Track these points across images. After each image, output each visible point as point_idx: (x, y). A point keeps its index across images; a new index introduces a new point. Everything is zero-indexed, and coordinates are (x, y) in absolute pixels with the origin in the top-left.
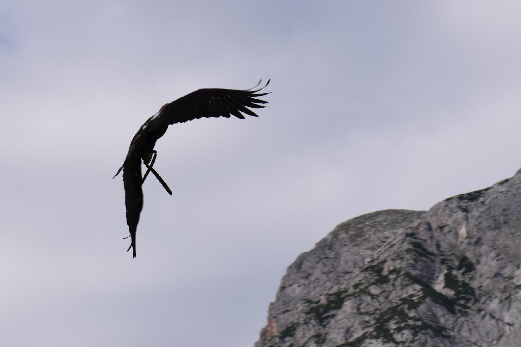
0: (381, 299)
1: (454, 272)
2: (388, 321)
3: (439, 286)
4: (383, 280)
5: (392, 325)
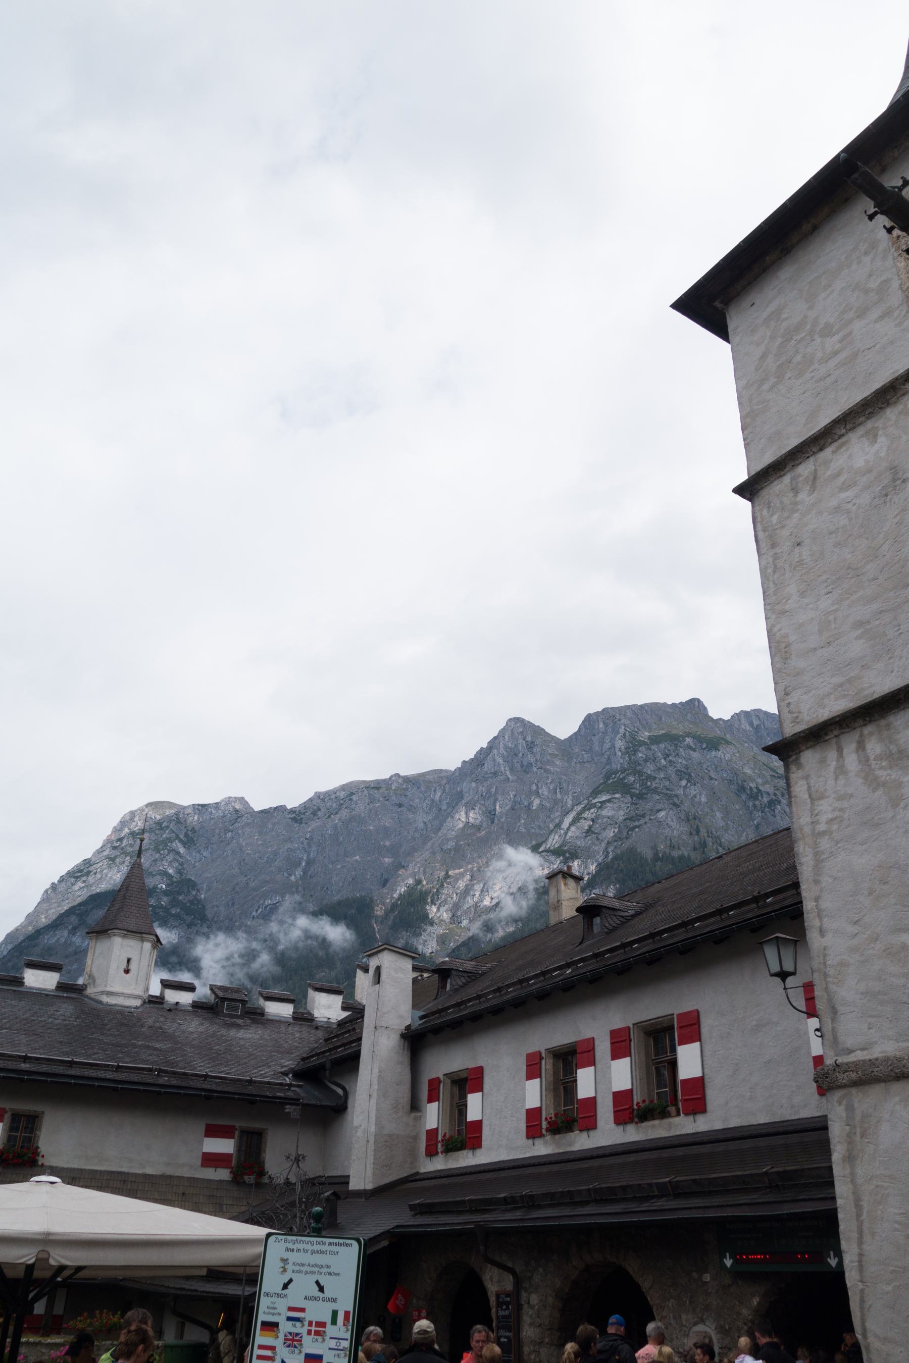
0: (159, 836)
1: (189, 832)
2: (160, 845)
4: (161, 829)
5: (161, 847)
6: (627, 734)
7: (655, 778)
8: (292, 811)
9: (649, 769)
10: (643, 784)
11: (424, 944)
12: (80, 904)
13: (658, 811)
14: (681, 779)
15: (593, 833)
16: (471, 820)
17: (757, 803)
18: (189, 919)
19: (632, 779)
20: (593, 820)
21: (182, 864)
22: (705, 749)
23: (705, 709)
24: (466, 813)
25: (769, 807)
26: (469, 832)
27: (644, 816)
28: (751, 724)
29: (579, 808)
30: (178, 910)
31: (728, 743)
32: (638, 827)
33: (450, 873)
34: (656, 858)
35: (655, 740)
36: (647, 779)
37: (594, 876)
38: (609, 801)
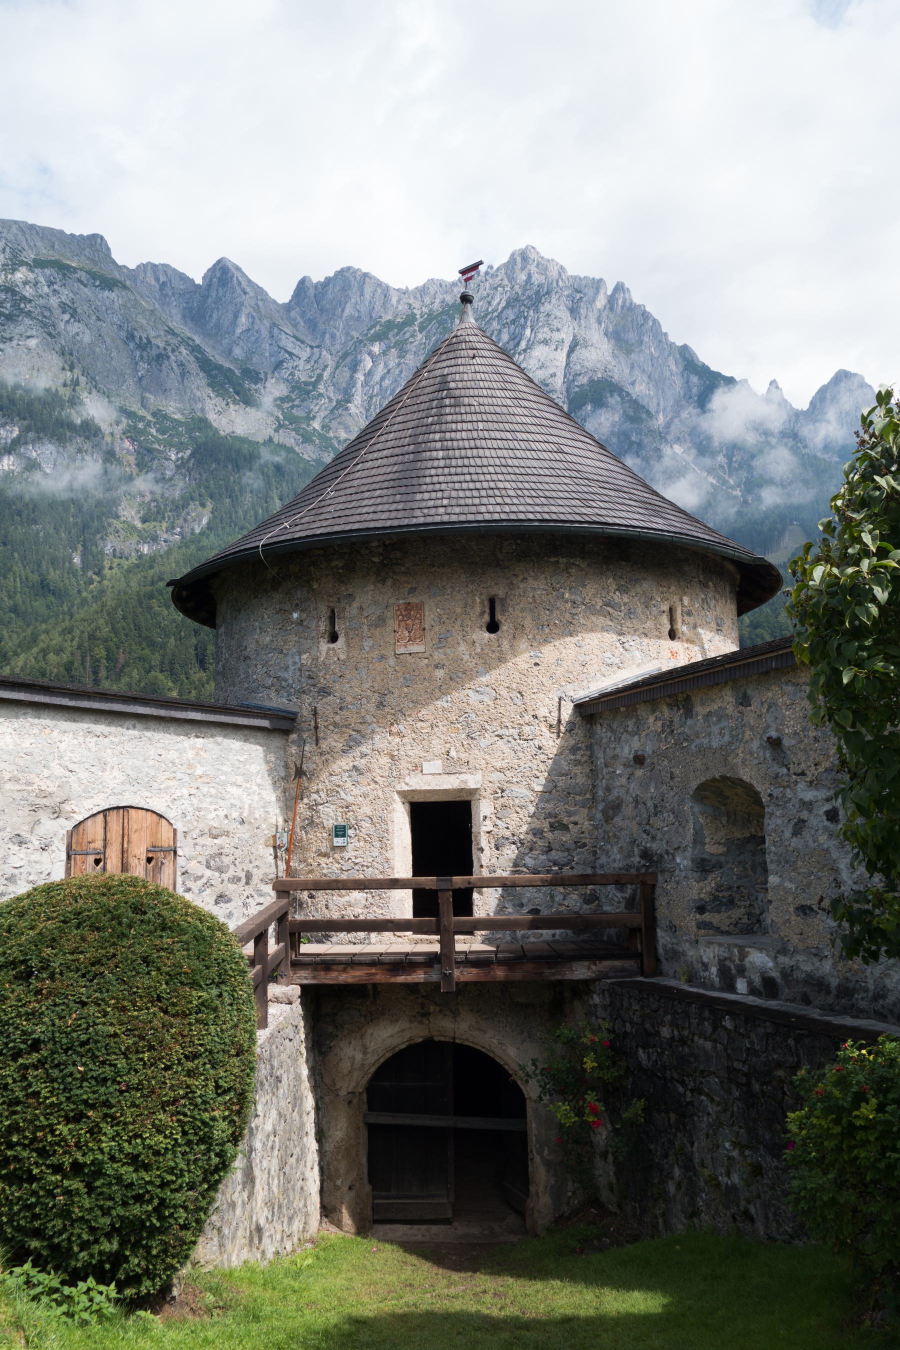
6: (8, 249)
7: (30, 301)
9: (28, 292)
10: (15, 305)
13: (28, 337)
14: (63, 313)
17: (145, 354)
23: (108, 249)
25: (157, 361)
27: (11, 339)
28: (157, 279)
31: (125, 287)
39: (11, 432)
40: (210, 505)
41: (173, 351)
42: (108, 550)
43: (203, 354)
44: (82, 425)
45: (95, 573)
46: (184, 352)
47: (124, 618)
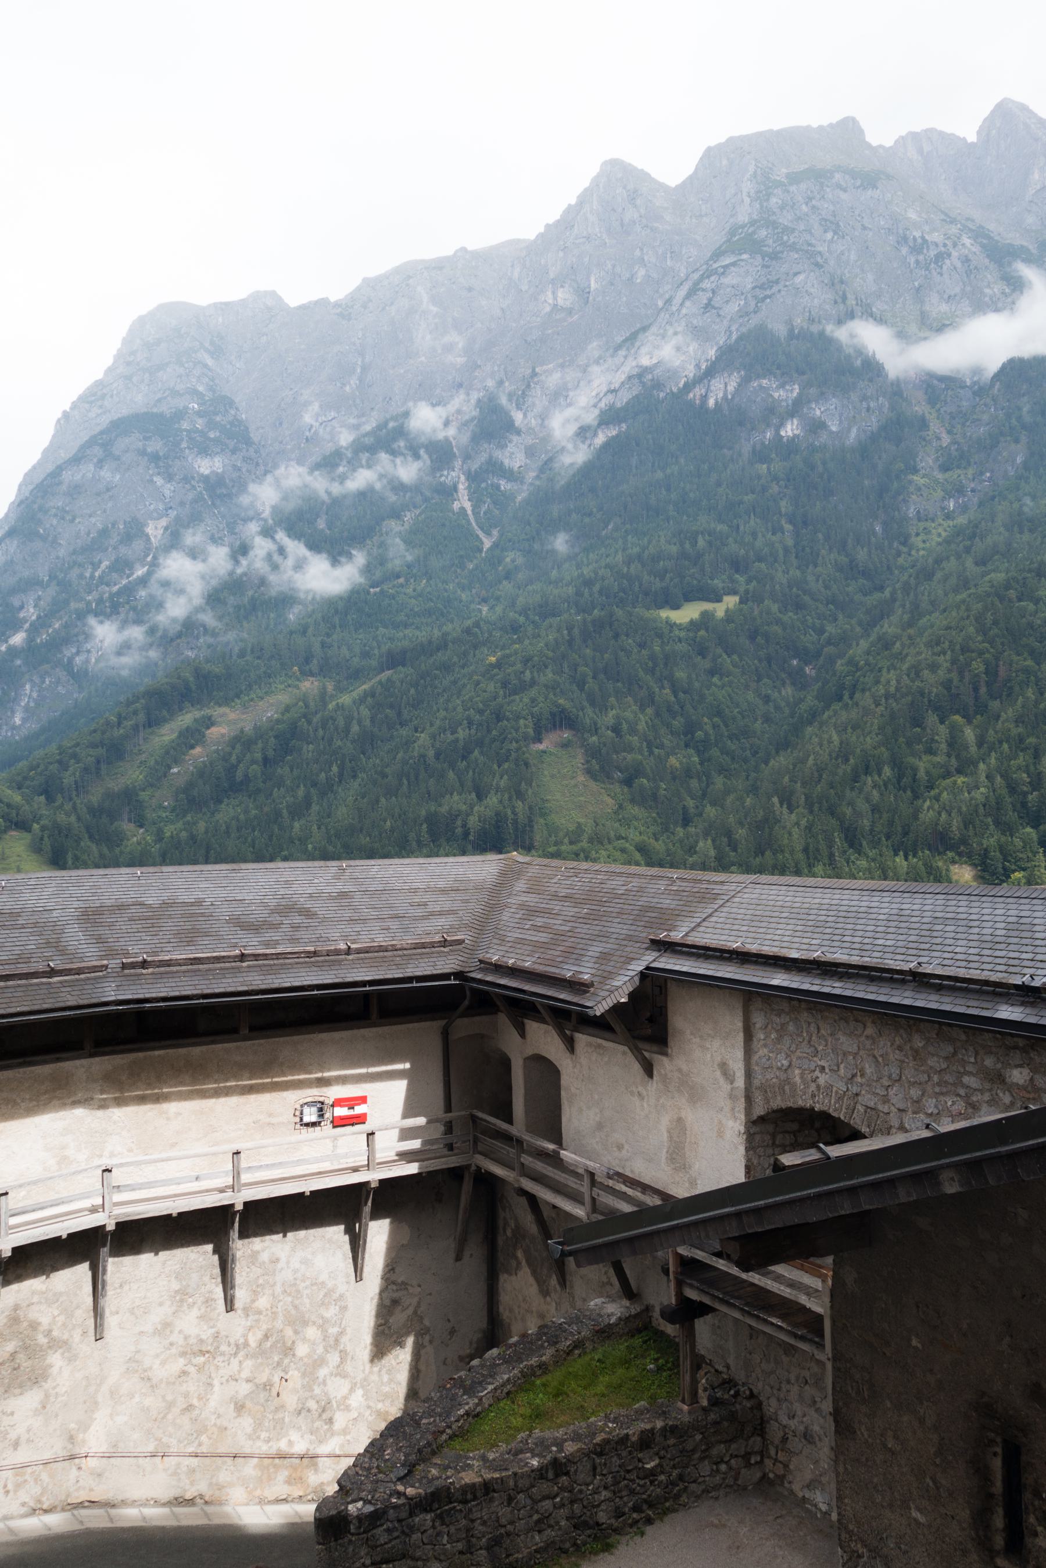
3: (207, 345)
7: (793, 230)
8: (337, 305)
9: (785, 219)
11: (511, 457)
12: (102, 433)
13: (796, 274)
14: (825, 231)
15: (714, 308)
16: (560, 302)
17: (921, 258)
18: (232, 444)
19: (763, 233)
20: (714, 292)
21: (213, 380)
22: (858, 187)
24: (553, 293)
25: (936, 263)
26: (558, 317)
27: (777, 282)
29: (696, 276)
30: (218, 434)
32: (769, 297)
33: (537, 370)
34: (791, 335)
35: (795, 178)
36: (783, 233)
37: (714, 364)
38: (734, 264)
39: (792, 391)
40: (1024, 439)
41: (955, 245)
42: (911, 512)
43: (989, 238)
44: (863, 364)
45: (901, 543)
46: (967, 242)
47: (995, 623)
